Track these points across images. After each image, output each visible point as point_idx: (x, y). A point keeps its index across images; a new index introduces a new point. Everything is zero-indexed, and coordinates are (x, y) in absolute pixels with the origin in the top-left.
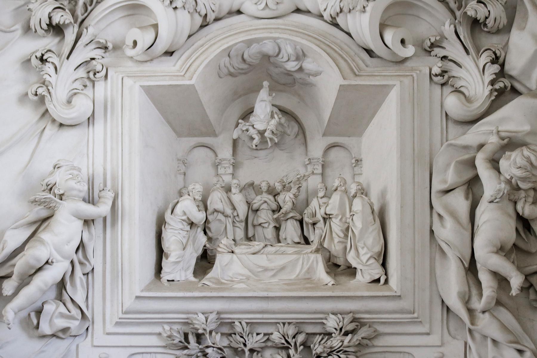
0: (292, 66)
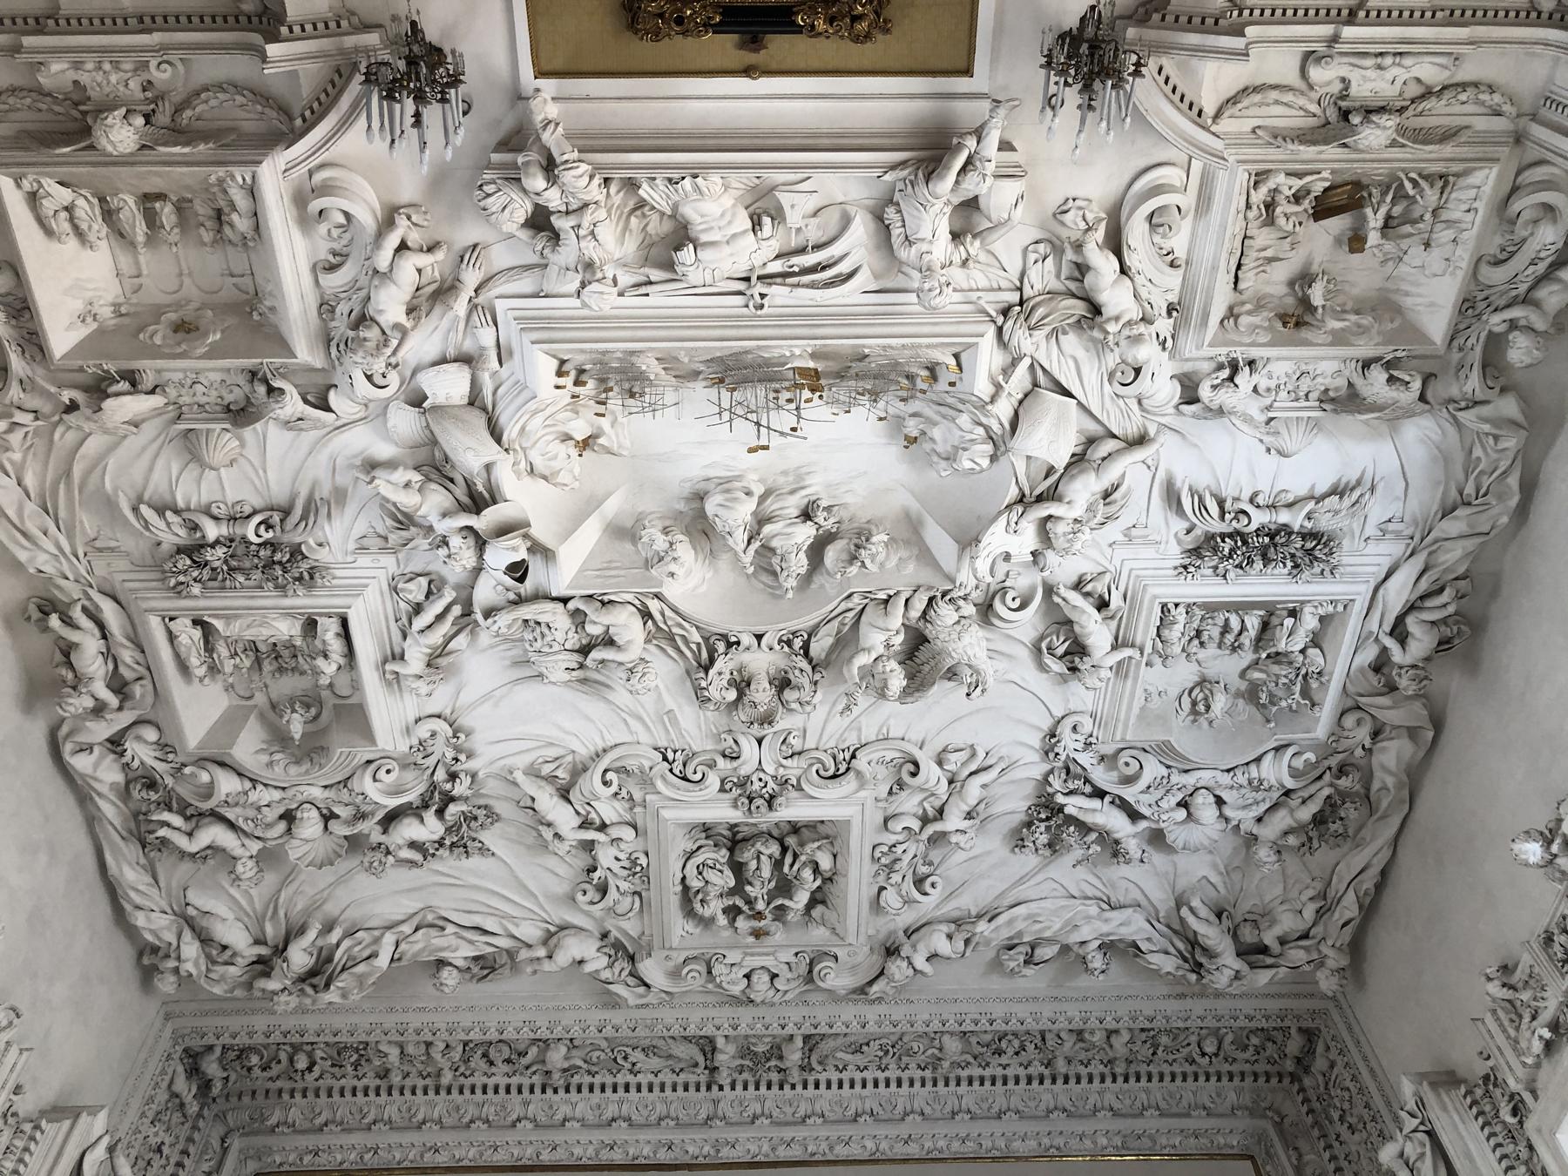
0: (277, 757)
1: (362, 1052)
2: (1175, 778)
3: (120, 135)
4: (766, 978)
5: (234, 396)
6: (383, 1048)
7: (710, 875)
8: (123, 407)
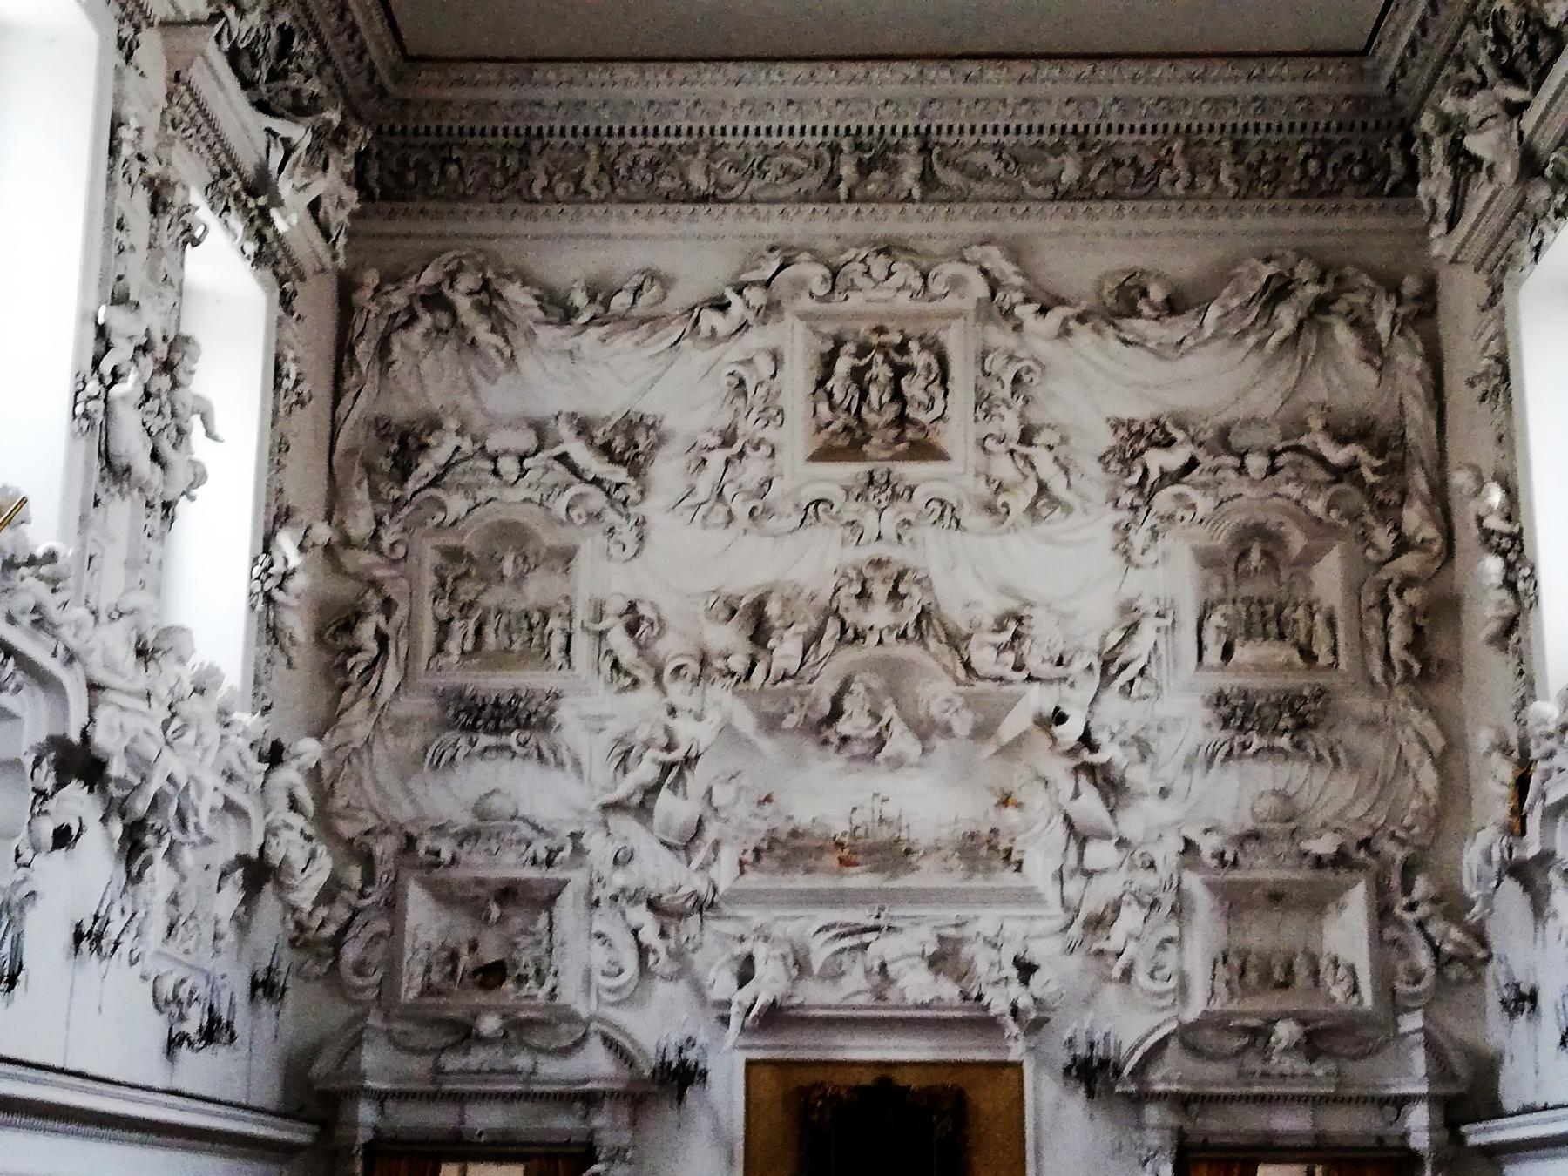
1: (1248, 187)
2: (536, 496)
3: (1285, 1032)
4: (875, 272)
5: (1251, 846)
6: (1232, 188)
7: (925, 398)
8: (1324, 846)
